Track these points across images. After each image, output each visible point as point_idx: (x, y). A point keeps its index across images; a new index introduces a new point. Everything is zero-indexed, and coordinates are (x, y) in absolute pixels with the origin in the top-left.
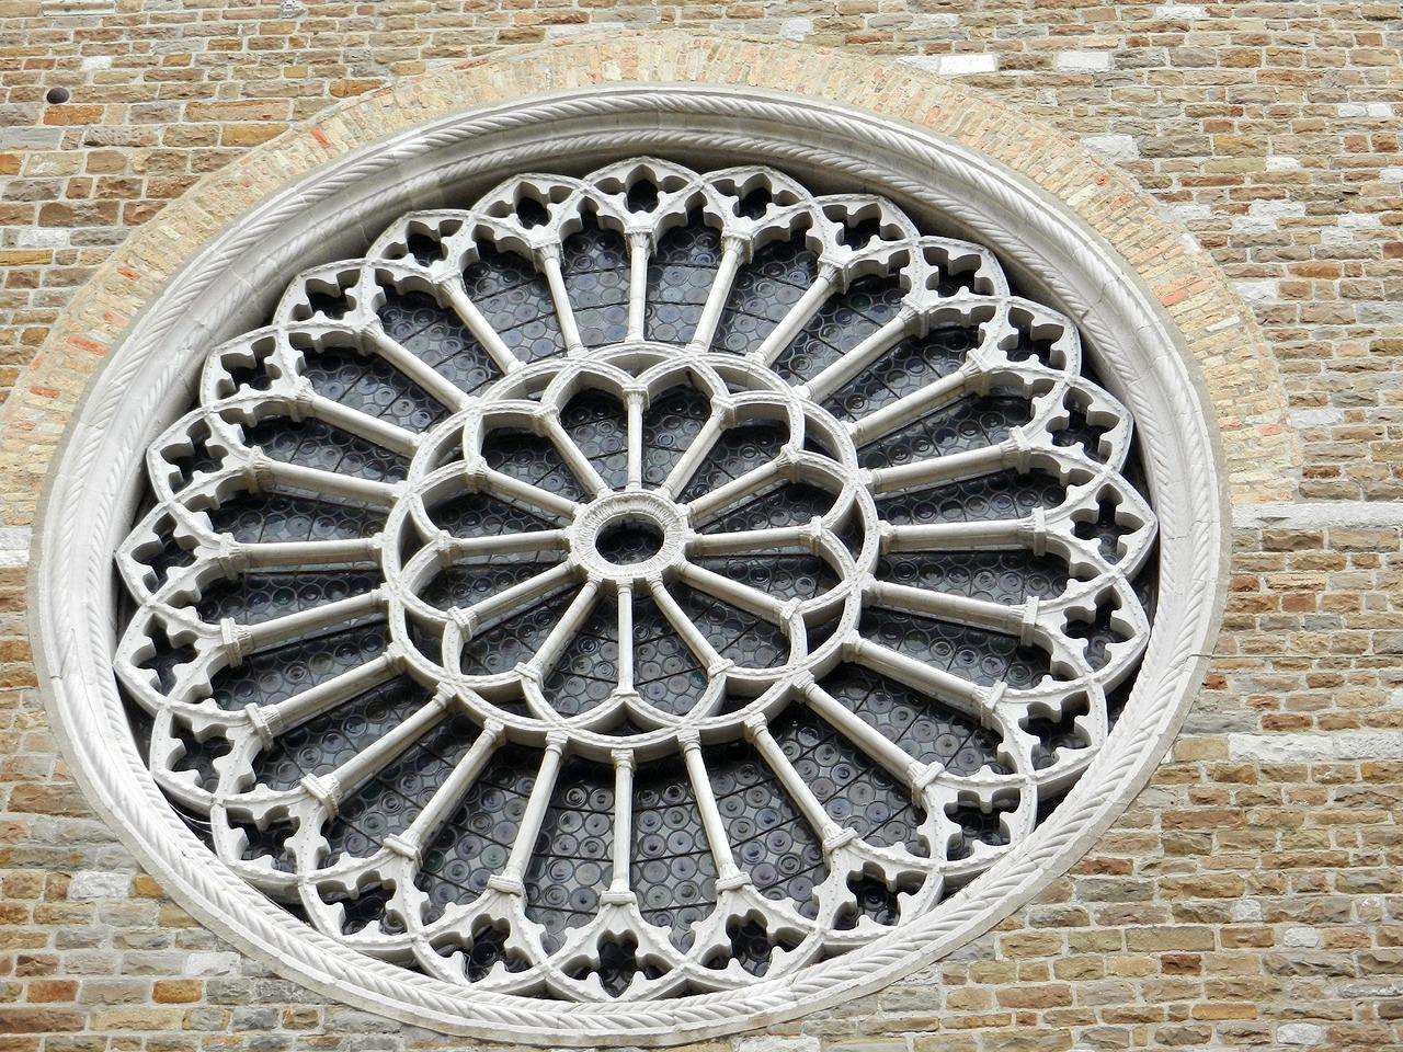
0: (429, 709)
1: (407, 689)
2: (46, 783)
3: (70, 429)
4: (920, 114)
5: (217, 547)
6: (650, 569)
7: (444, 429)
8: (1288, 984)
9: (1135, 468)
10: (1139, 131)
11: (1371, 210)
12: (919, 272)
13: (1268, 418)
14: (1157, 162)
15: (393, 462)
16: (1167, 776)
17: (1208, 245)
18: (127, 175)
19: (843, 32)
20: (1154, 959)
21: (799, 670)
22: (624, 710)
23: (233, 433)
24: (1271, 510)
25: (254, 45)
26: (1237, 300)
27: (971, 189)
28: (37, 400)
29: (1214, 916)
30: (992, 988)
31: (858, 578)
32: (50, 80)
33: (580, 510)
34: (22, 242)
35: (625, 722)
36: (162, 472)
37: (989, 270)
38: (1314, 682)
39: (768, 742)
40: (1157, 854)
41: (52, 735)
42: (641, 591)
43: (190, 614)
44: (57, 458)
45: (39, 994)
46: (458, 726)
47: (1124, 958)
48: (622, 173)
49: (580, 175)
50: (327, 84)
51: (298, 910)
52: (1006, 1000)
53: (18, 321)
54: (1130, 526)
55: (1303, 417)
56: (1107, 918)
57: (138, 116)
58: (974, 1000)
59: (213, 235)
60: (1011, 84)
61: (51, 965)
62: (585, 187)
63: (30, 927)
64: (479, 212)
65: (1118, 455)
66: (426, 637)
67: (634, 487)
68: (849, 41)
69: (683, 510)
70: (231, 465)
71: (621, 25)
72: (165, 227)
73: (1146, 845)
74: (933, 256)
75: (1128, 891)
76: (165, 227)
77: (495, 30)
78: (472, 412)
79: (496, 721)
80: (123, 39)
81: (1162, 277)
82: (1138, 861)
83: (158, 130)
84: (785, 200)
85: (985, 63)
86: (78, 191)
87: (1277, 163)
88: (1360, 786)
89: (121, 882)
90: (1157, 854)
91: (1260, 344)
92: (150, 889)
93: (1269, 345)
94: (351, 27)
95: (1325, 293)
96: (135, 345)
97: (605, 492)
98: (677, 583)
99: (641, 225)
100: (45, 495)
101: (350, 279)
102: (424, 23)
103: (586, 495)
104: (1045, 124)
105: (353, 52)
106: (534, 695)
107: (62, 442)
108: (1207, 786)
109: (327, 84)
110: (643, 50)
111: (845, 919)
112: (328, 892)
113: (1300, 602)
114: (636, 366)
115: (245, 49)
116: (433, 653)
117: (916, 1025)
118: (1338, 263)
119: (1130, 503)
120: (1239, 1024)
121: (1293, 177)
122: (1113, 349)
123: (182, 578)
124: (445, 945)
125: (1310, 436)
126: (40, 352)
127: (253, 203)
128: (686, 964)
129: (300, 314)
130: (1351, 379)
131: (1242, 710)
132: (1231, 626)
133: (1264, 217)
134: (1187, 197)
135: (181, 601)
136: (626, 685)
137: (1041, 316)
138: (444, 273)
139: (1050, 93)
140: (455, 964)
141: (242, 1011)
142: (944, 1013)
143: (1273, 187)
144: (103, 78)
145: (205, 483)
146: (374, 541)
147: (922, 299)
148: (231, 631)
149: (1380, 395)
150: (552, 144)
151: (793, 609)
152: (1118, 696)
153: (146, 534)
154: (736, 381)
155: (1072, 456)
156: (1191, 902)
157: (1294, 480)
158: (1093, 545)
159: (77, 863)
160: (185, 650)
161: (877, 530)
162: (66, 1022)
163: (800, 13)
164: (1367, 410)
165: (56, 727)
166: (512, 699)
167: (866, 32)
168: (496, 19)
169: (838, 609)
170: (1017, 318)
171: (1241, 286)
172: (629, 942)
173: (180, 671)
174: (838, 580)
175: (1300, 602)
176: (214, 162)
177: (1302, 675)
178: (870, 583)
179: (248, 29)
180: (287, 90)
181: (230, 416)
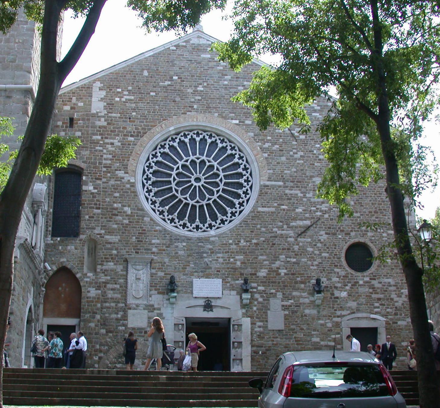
0: (177, 200)
1: (174, 197)
2: (140, 207)
3: (137, 165)
4: (230, 128)
5: (154, 179)
6: (200, 184)
7: (177, 165)
8: (262, 234)
9: (251, 174)
10: (254, 132)
11: (278, 145)
12: (229, 148)
13: (265, 171)
14: (256, 137)
15: (172, 169)
16: (252, 212)
17: (260, 148)
18: (139, 131)
19: (221, 116)
20: (250, 231)
21: (215, 197)
22: (198, 201)
23: (153, 164)
24: (264, 182)
25: (152, 112)
26: (263, 156)
27: (235, 139)
28: (133, 161)
29: (255, 227)
30: (234, 233)
31: (221, 187)
32: (129, 116)
33: (192, 177)
34: (128, 139)
35: (198, 202)
36: (146, 169)
37: (236, 148)
38: (267, 202)
39: (212, 204)
40: (251, 220)
41: (140, 202)
42: (199, 187)
43: (151, 187)
44: (136, 169)
45: (143, 230)
46: (180, 201)
47: (247, 231)
48: (196, 132)
49: (191, 132)
50: (162, 119)
51: (166, 221)
52: (235, 234)
53: (129, 150)
54: (250, 181)
55: (269, 171)
56: (245, 227)
57: (140, 122)
58: (232, 234)
59: (151, 140)
60: (240, 125)
61: (143, 228)
62: (191, 134)
63: (140, 223)
64: (179, 137)
65: (249, 173)
66: (177, 191)
67: (198, 174)
68: (222, 117)
69: (203, 177)
70: (154, 169)
71: (195, 113)
72: (145, 138)
73: (249, 219)
74: (231, 146)
75: (248, 224)
76: (145, 138)
77: (181, 112)
78: (180, 163)
79: (185, 201)
80: (137, 110)
81: (255, 152)
82: (249, 221)
83: (142, 124)
84: (214, 137)
85: (237, 122)
86: (134, 132)
87: (269, 138)
88: (270, 214)
89: (149, 219)
90: (251, 220)
91: (265, 162)
92: (152, 219)
93: (266, 162)
94: (164, 110)
95: (272, 156)
96: (143, 154)
97: (195, 175)
98: (202, 185)
99: (198, 139)
100: (135, 173)
101: (165, 144)
102: (173, 111)
103: (193, 175)
104: (244, 131)
105: (165, 114)
106: (188, 199)
107: (136, 166)
108: (256, 213)
109: (162, 119)
110: (198, 117)
111: (220, 224)
112: (169, 219)
113: (266, 193)
114: (198, 159)
115: (151, 113)
116: (177, 193)
117: (227, 237)
118: (274, 152)
119: (250, 179)
120: (257, 238)
121: (270, 140)
122: (249, 160)
123: (150, 182)
124: (180, 225)
125: (269, 174)
126: (132, 154)
127: (155, 136)
128: (204, 228)
129: (160, 149)
130: (274, 167)
131: (260, 205)
132: (259, 196)
133: (267, 145)
134: (258, 142)
135: (150, 185)
136: (198, 198)
137: (242, 155)
138: (176, 144)
139: (244, 127)
140: (181, 228)
141: (162, 233)
142: (230, 236)
143: (268, 141)
144: (135, 116)
145: (151, 170)
146: (170, 179)
147: (229, 152)
148: (156, 189)
149: (277, 169)
150: (188, 128)
151: (215, 190)
152: (248, 201)
153: (145, 177)
154: (209, 161)
155: (244, 172)
156: (253, 225)
157: (267, 179)
158: (246, 183)
159: (144, 217)
160: (151, 191)
161: (224, 181)
162: (145, 233)
163: (216, 113)
164: (275, 171)
165: (140, 201)
166: (186, 199)
167: (224, 116)
168: (181, 111)
169: (219, 190)
170: (239, 155)
171: (264, 154)
172: (198, 226)
173: (151, 193)
174: (219, 186)
175: (266, 193)
176: (150, 129)
177: (266, 202)
178: (223, 187)
179: (152, 110)
180: (158, 120)
181: (153, 162)
